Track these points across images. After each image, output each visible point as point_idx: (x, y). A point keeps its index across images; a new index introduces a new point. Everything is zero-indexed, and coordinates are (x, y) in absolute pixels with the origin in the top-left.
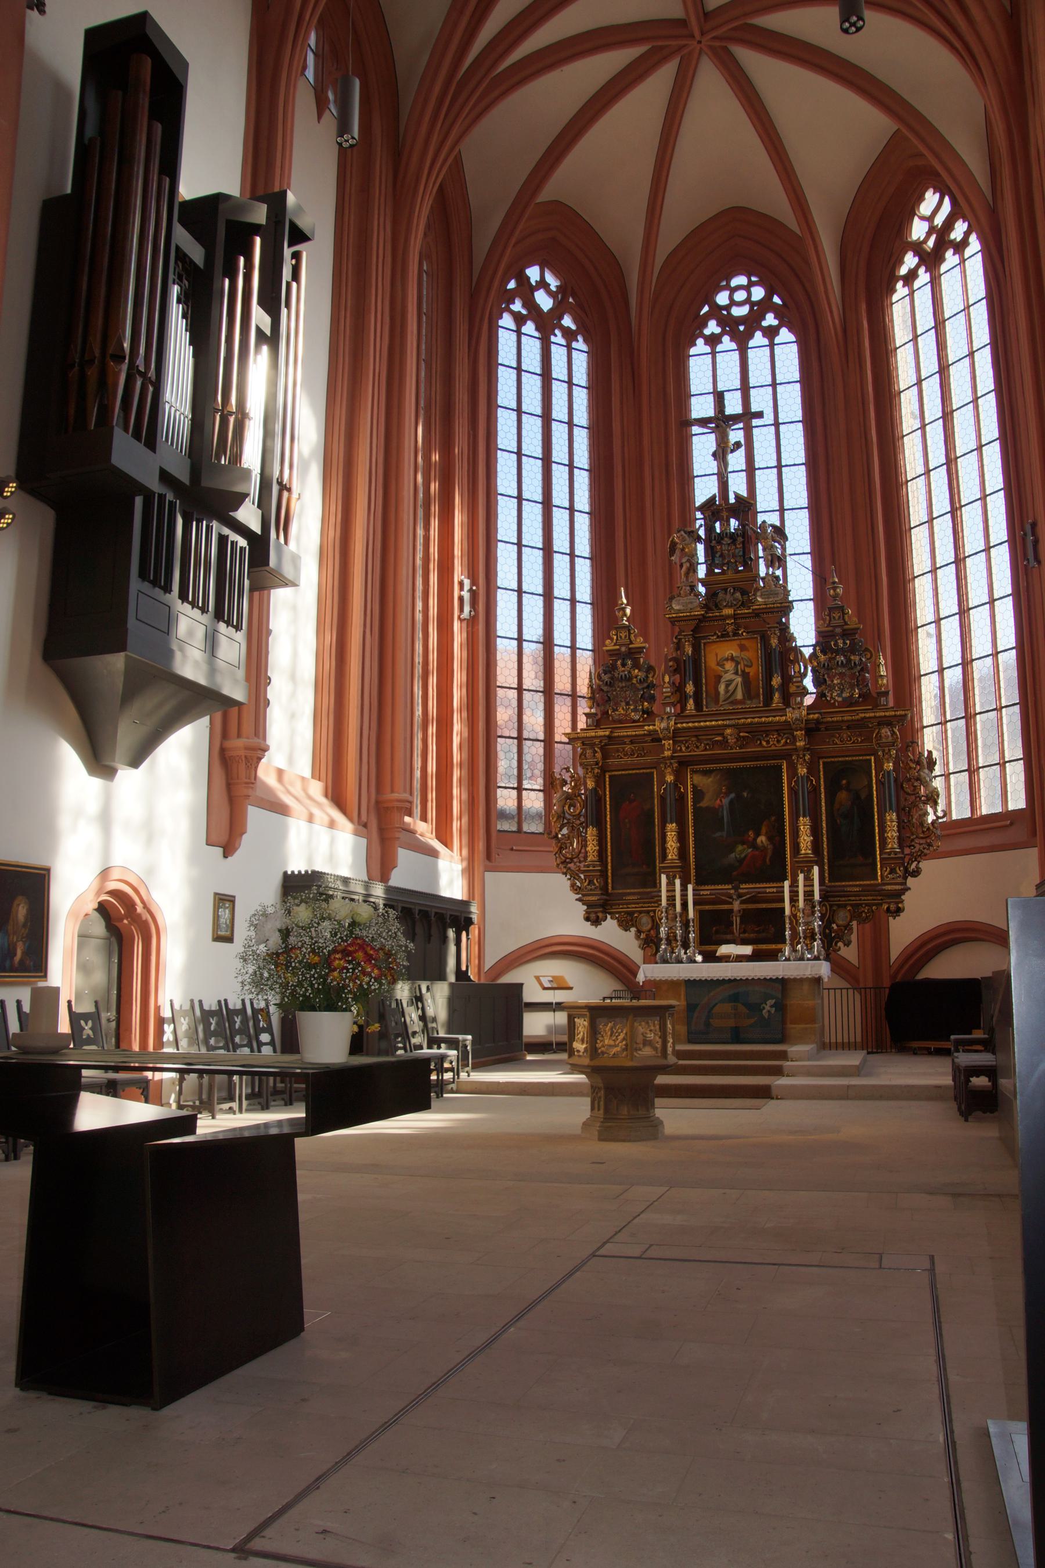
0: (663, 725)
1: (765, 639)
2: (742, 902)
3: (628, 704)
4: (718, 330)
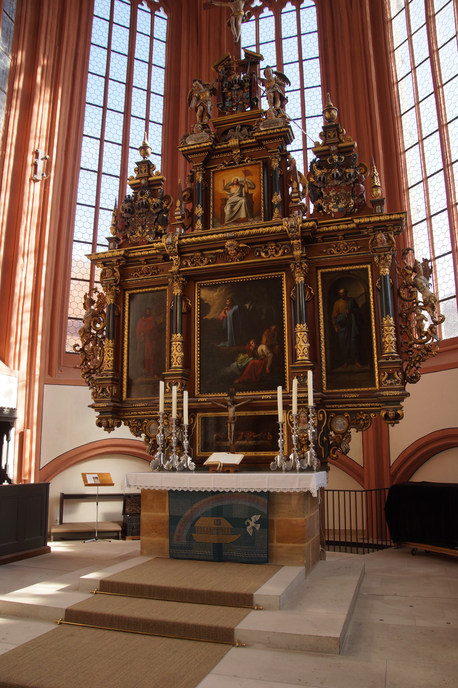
0: (169, 240)
1: (267, 165)
2: (237, 410)
3: (143, 227)
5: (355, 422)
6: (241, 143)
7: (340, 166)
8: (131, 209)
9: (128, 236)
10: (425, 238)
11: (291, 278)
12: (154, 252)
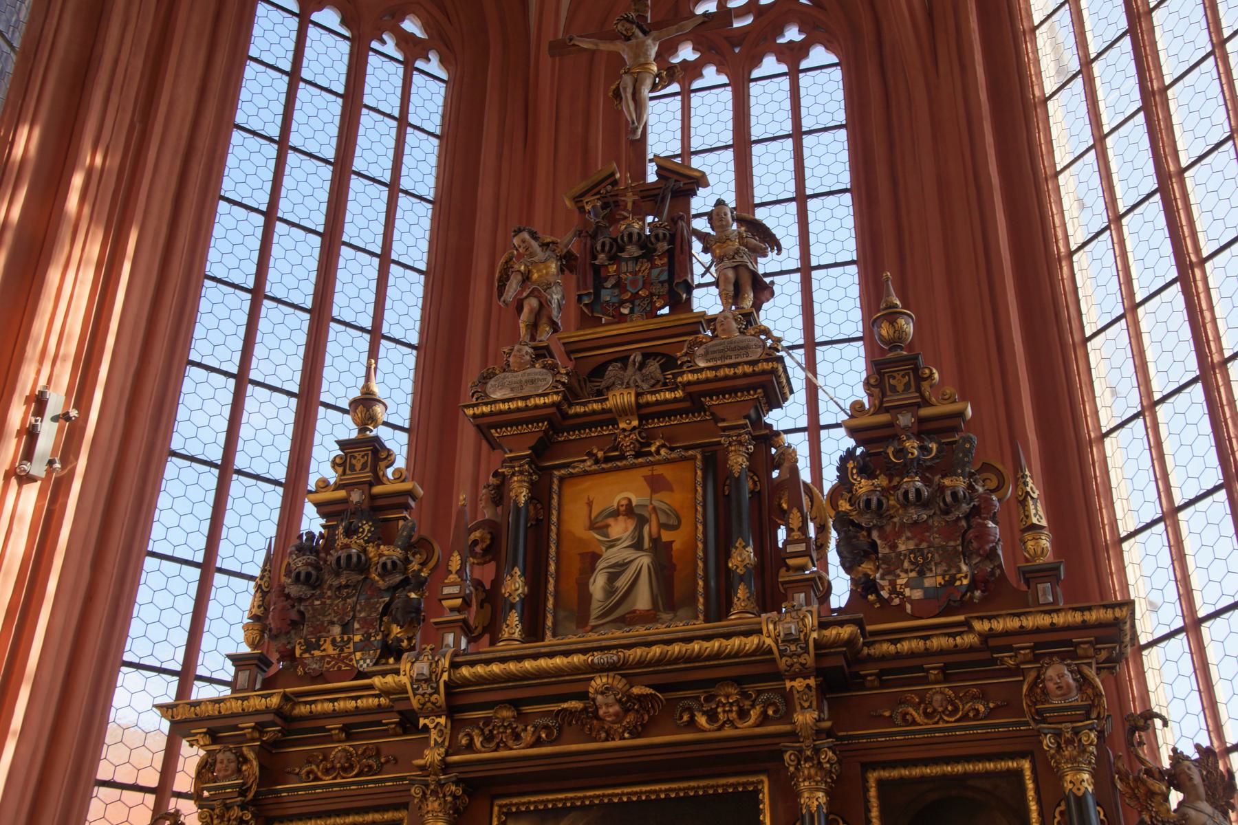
0: (423, 667)
1: (714, 461)
3: (346, 627)
6: (643, 400)
7: (925, 470)
8: (313, 572)
9: (297, 655)
10: (1188, 685)
11: (787, 794)
12: (372, 702)
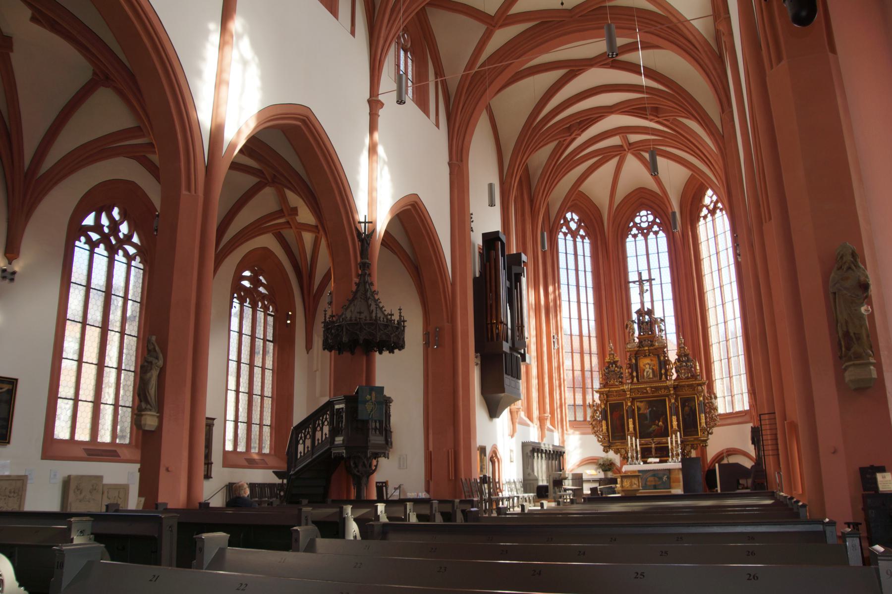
4: (636, 232)
5: (693, 447)
11: (670, 400)
